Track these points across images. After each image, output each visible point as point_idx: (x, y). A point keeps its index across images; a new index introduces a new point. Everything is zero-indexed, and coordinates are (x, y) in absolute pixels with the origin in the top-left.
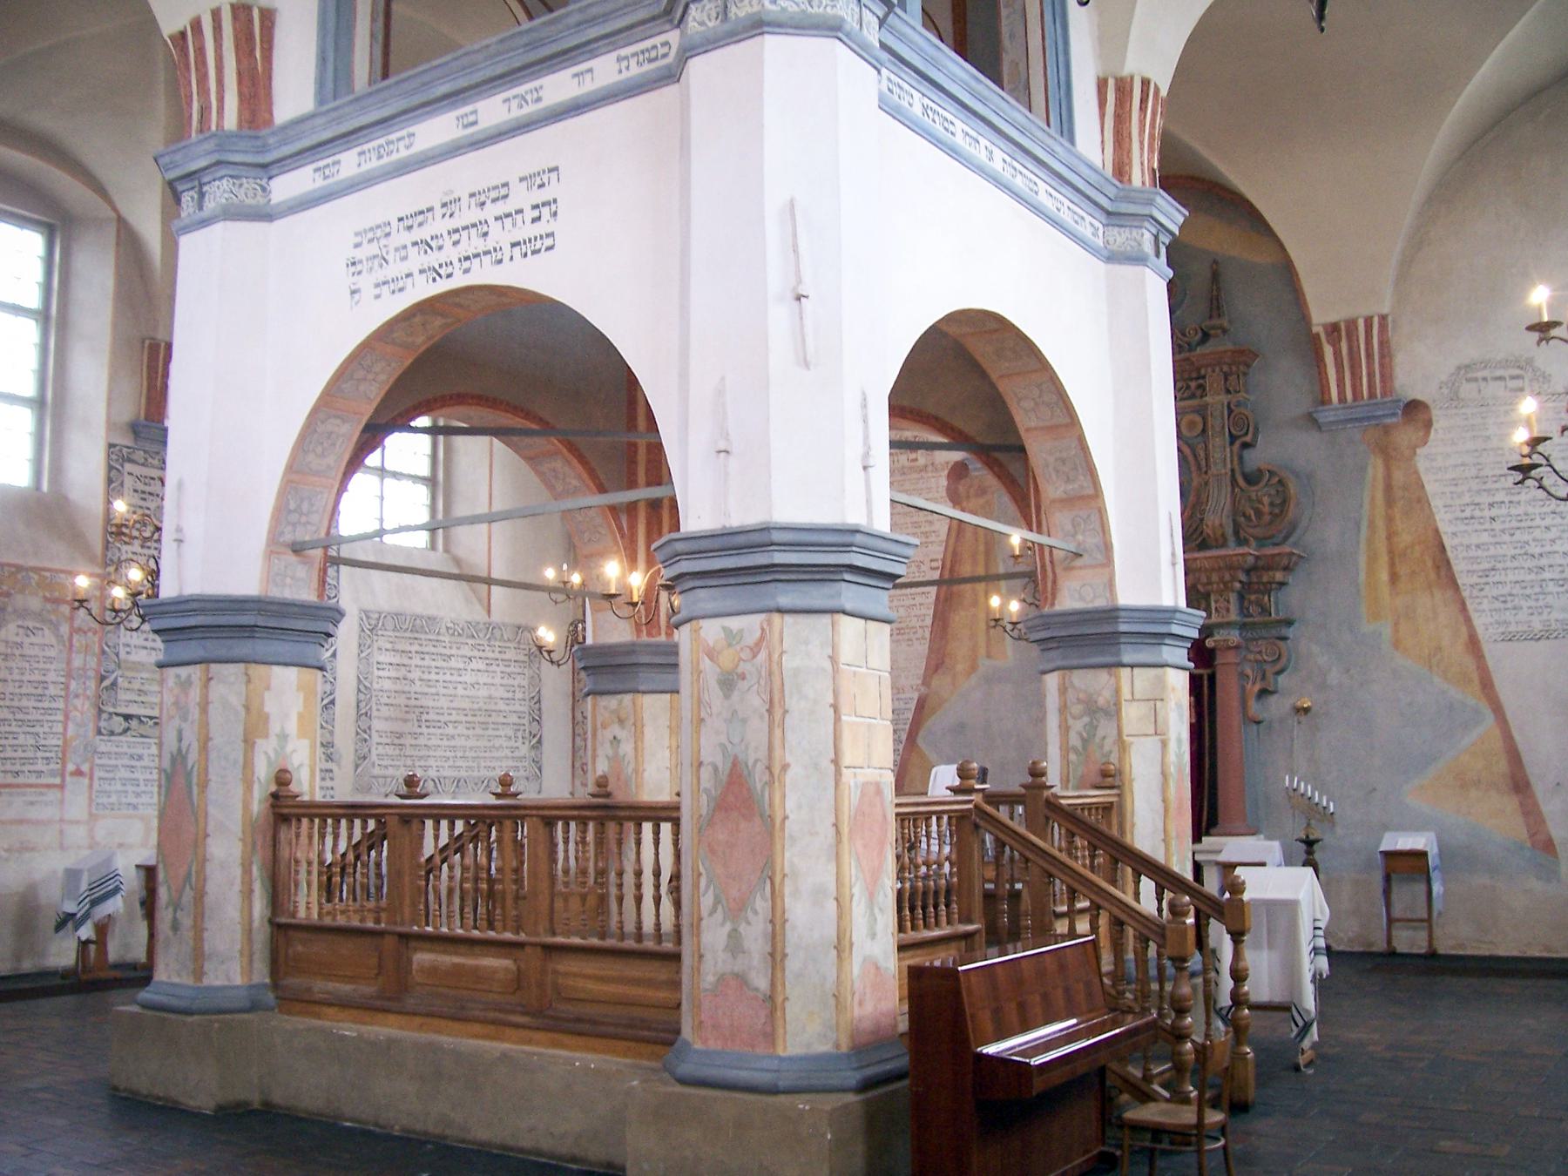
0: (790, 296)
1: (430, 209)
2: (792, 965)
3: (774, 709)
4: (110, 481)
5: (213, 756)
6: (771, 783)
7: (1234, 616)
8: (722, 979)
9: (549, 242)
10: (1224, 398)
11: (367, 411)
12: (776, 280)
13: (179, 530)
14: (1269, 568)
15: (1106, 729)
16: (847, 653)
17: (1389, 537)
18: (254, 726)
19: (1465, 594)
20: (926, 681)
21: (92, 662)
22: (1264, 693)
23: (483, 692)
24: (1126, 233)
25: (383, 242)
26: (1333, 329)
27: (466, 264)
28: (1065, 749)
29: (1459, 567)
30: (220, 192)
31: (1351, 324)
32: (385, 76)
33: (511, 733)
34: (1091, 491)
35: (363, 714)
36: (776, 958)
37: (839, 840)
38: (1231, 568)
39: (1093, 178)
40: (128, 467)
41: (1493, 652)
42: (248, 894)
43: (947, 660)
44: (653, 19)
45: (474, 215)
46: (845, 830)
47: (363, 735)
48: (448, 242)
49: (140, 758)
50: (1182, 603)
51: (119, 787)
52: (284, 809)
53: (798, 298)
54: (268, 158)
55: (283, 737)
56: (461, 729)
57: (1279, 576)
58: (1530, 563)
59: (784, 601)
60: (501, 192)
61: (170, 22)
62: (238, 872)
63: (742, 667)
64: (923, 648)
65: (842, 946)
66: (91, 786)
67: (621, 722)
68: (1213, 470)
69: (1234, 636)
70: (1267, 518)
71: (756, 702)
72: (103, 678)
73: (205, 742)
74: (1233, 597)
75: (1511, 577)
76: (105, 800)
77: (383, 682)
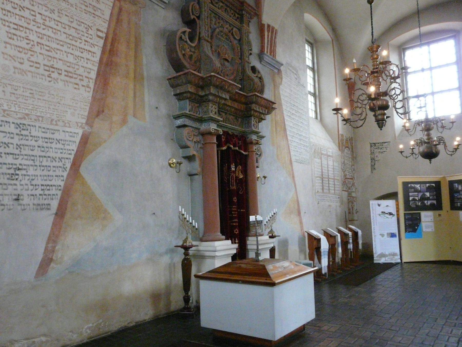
19: (289, 142)
20: (90, 122)
29: (288, 133)
41: (294, 164)
43: (106, 111)
58: (299, 137)
64: (88, 95)
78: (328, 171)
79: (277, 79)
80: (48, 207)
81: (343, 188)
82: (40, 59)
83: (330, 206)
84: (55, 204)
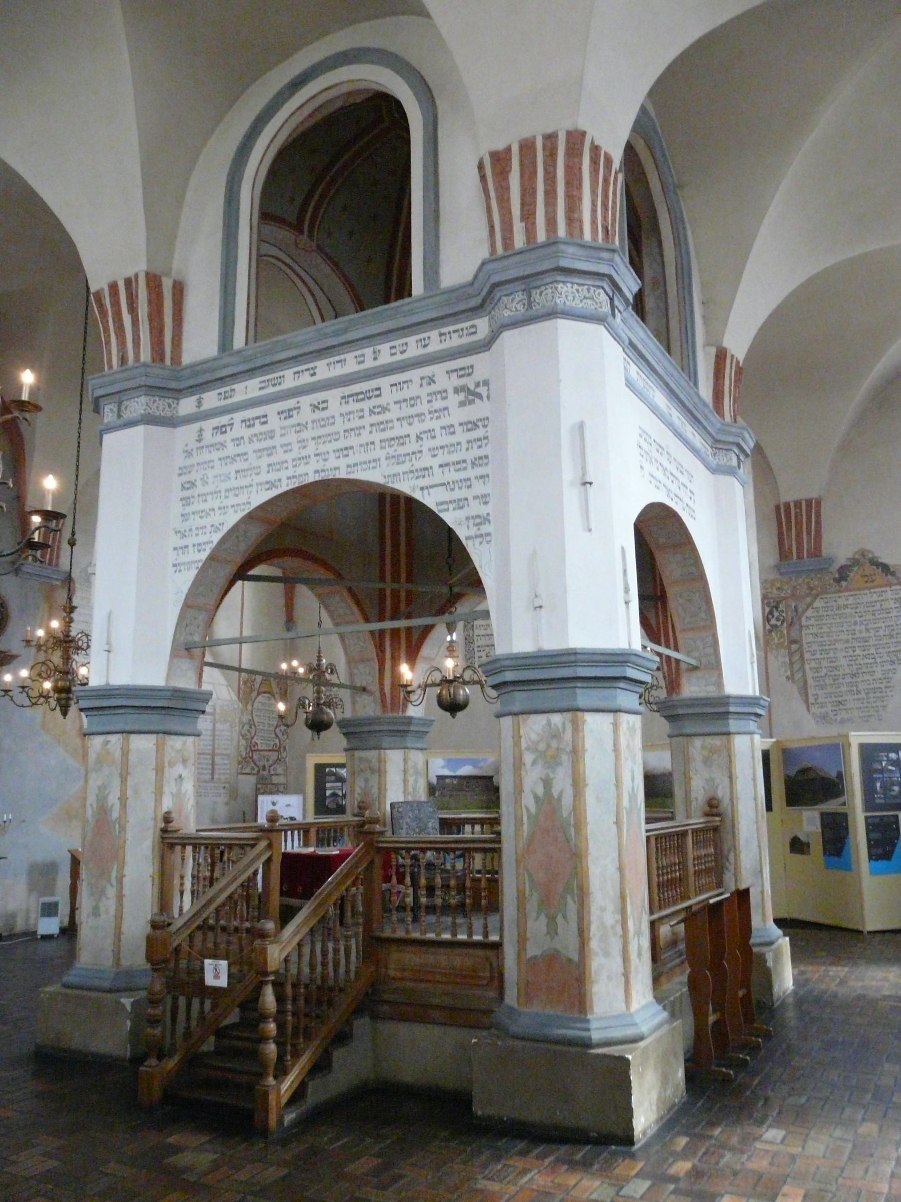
81: (242, 768)
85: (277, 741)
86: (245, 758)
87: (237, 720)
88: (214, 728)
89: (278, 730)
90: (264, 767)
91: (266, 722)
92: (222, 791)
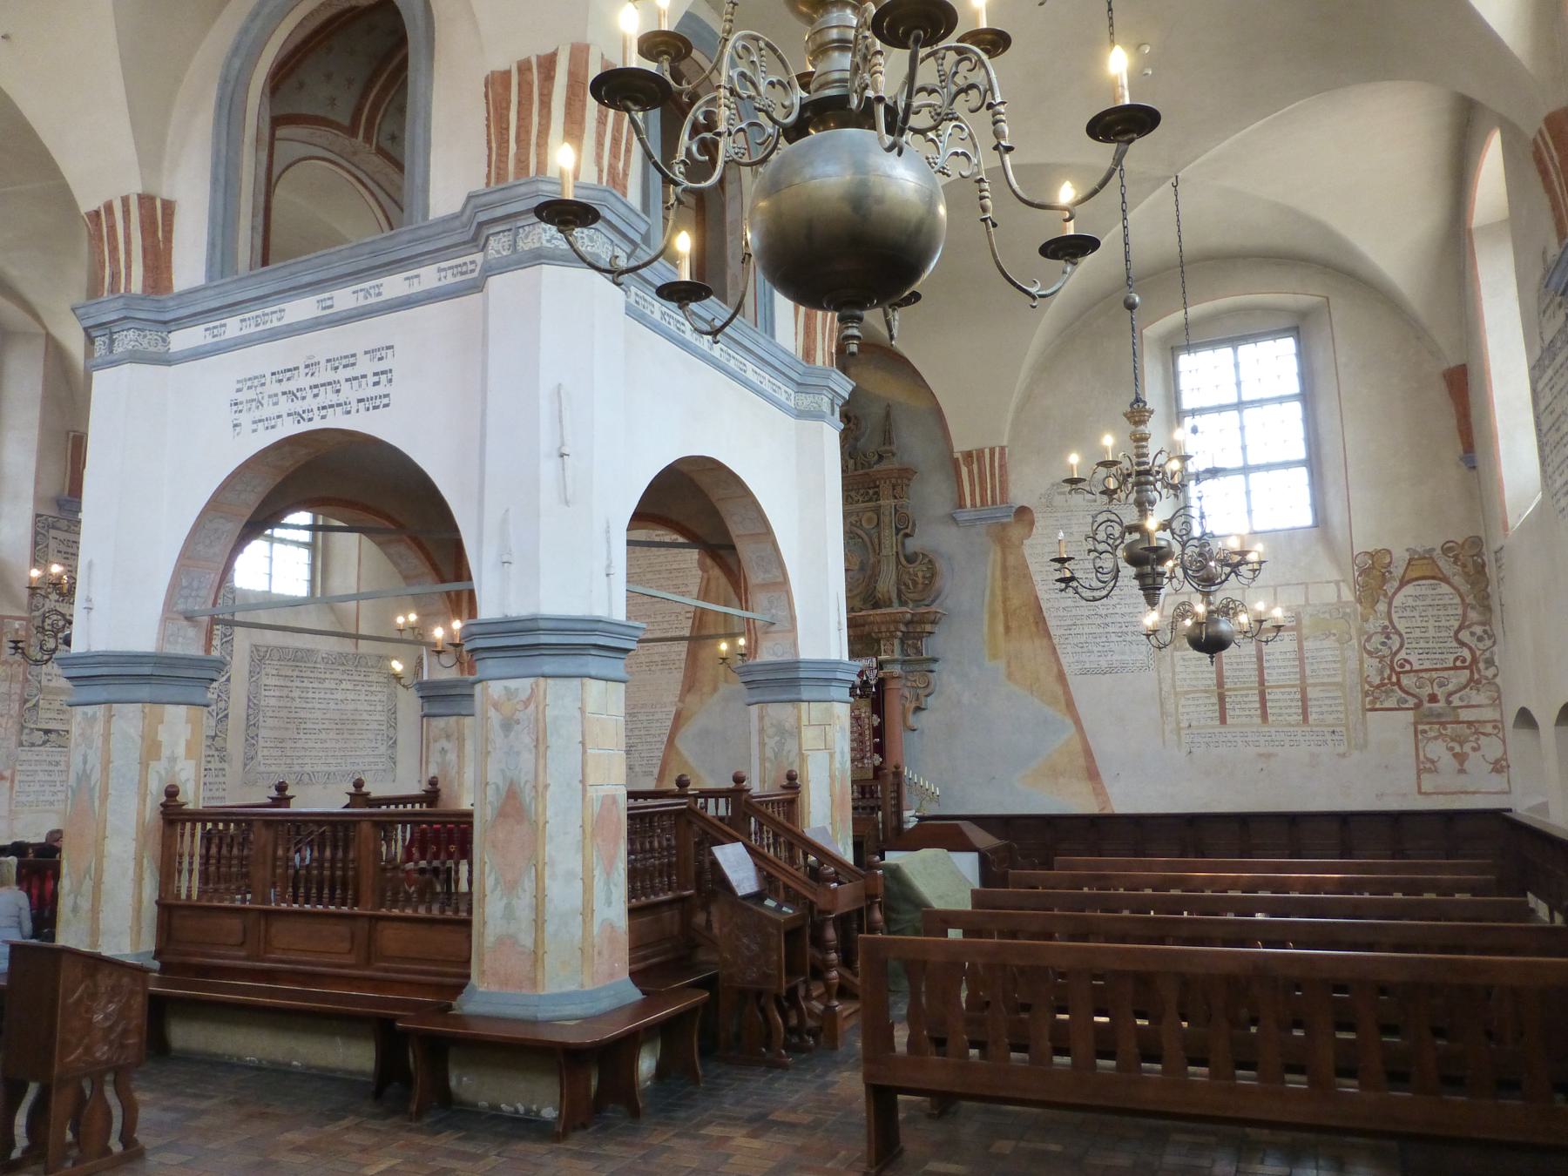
0: (556, 454)
1: (296, 368)
2: (550, 928)
3: (540, 744)
4: (36, 544)
5: (112, 775)
6: (536, 798)
7: (897, 655)
8: (501, 941)
9: (385, 401)
10: (892, 502)
11: (247, 514)
12: (546, 442)
13: (89, 600)
14: (922, 622)
15: (791, 745)
16: (591, 707)
17: (1005, 600)
18: (151, 749)
20: (681, 700)
21: (16, 688)
22: (918, 709)
23: (351, 706)
24: (810, 398)
25: (259, 389)
26: (969, 455)
27: (323, 412)
28: (763, 760)
29: (1052, 623)
30: (127, 340)
31: (981, 452)
32: (265, 262)
33: (371, 736)
34: (781, 579)
35: (251, 725)
36: (539, 922)
37: (584, 838)
38: (896, 622)
39: (787, 360)
40: (53, 533)
42: (139, 881)
44: (464, 243)
45: (330, 376)
46: (589, 829)
47: (251, 740)
48: (309, 394)
49: (57, 763)
50: (846, 657)
51: (37, 788)
52: (173, 813)
53: (562, 455)
54: (168, 317)
55: (173, 759)
56: (332, 735)
57: (928, 628)
59: (547, 669)
60: (350, 361)
61: (87, 204)
62: (131, 865)
63: (519, 715)
64: (679, 676)
65: (587, 911)
66: (12, 788)
67: (448, 737)
68: (884, 552)
69: (897, 669)
70: (920, 586)
71: (527, 740)
72: (26, 701)
73: (106, 763)
74: (896, 642)
75: (1087, 630)
76: (23, 798)
77: (269, 700)
78: (1261, 670)
79: (1015, 532)
80: (651, 773)
81: (1373, 702)
82: (643, 659)
83: (1269, 756)
84: (656, 771)
85: (1466, 653)
86: (1378, 687)
87: (1353, 632)
88: (1301, 648)
89: (1460, 636)
90: (1433, 698)
91: (1431, 623)
92: (1329, 737)
